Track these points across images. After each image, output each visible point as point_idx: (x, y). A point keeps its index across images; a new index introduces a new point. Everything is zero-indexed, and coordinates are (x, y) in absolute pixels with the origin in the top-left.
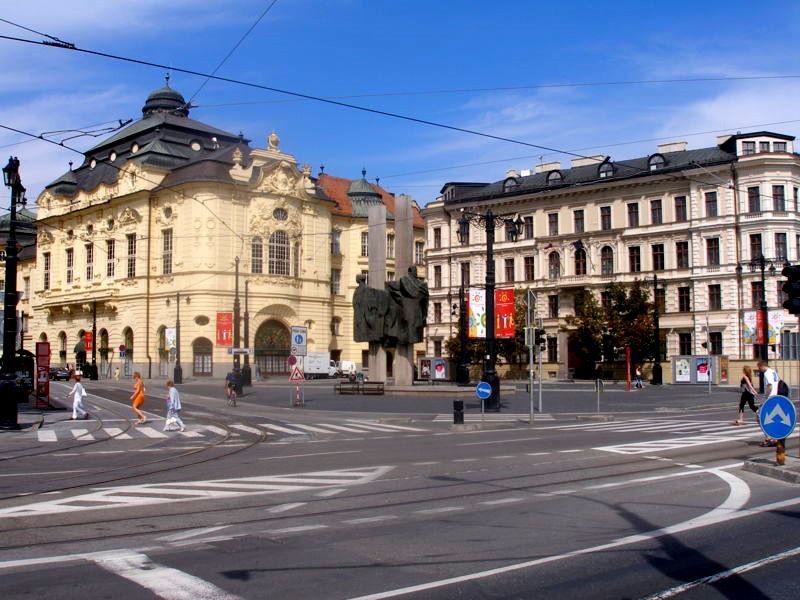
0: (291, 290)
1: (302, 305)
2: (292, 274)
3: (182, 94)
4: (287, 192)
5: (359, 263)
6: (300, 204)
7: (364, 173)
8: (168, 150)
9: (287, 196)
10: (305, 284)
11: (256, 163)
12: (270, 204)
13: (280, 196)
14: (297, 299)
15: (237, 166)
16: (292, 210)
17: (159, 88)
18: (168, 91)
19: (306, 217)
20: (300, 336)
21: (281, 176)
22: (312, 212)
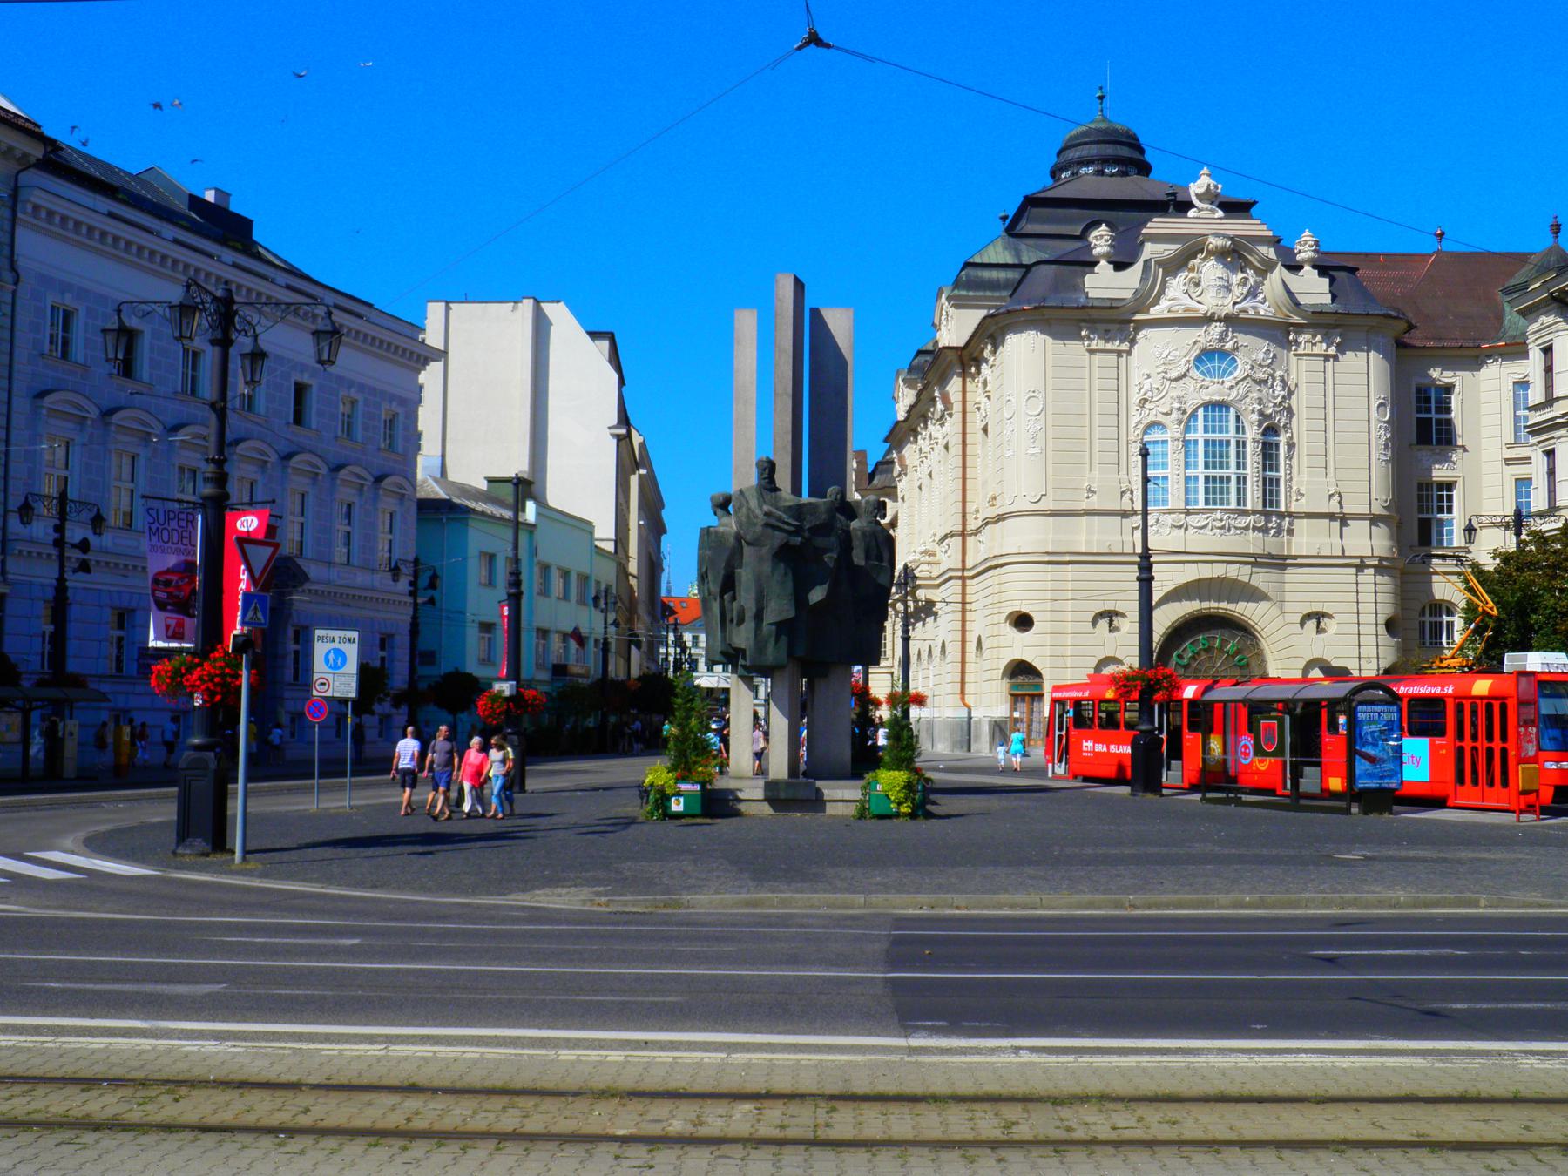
0: (1253, 543)
1: (1291, 575)
2: (1253, 499)
3: (1135, 129)
4: (1228, 309)
5: (1509, 462)
6: (1278, 332)
7: (1556, 229)
8: (1018, 254)
9: (1232, 321)
10: (1301, 525)
11: (1149, 250)
12: (1189, 340)
13: (1208, 319)
14: (1278, 562)
15: (1104, 267)
16: (1254, 349)
17: (1088, 118)
18: (1103, 125)
19: (1304, 362)
20: (338, 652)
21: (1211, 271)
22: (1321, 348)
